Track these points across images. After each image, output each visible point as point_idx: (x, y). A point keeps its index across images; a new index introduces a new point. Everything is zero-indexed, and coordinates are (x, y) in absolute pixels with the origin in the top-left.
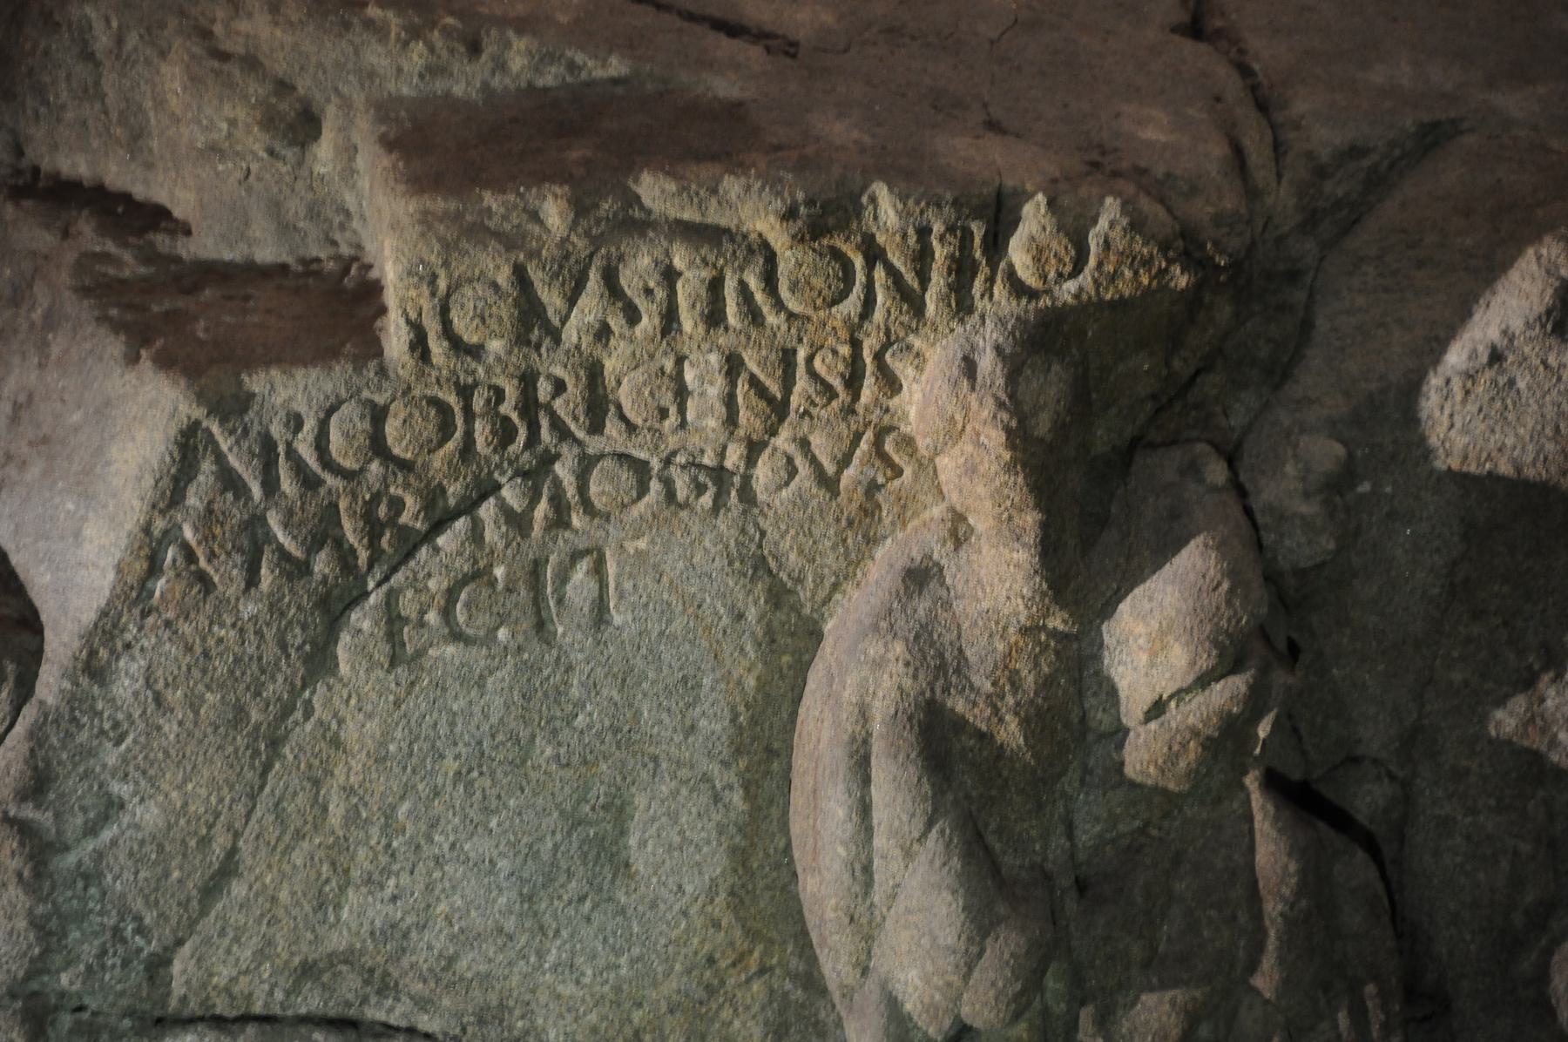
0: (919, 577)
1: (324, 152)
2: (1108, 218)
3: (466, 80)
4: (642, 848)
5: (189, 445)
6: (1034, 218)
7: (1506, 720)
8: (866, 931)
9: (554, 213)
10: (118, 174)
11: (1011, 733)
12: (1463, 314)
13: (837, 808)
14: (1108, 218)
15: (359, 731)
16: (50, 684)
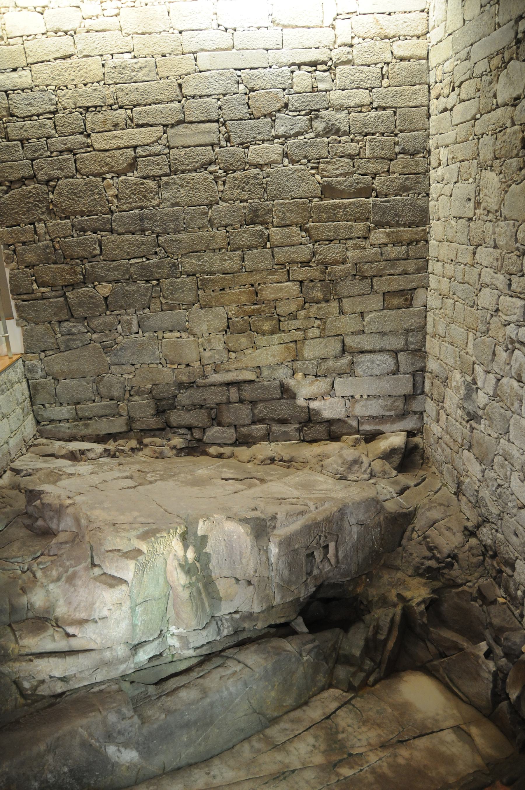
0: (175, 555)
1: (132, 541)
2: (182, 527)
3: (138, 533)
4: (160, 581)
5: (136, 564)
6: (179, 528)
7: (204, 551)
8: (178, 580)
9: (153, 539)
10: (114, 548)
11: (184, 563)
12: (198, 525)
13: (175, 573)
14: (182, 527)
15: (146, 580)
16: (130, 585)
